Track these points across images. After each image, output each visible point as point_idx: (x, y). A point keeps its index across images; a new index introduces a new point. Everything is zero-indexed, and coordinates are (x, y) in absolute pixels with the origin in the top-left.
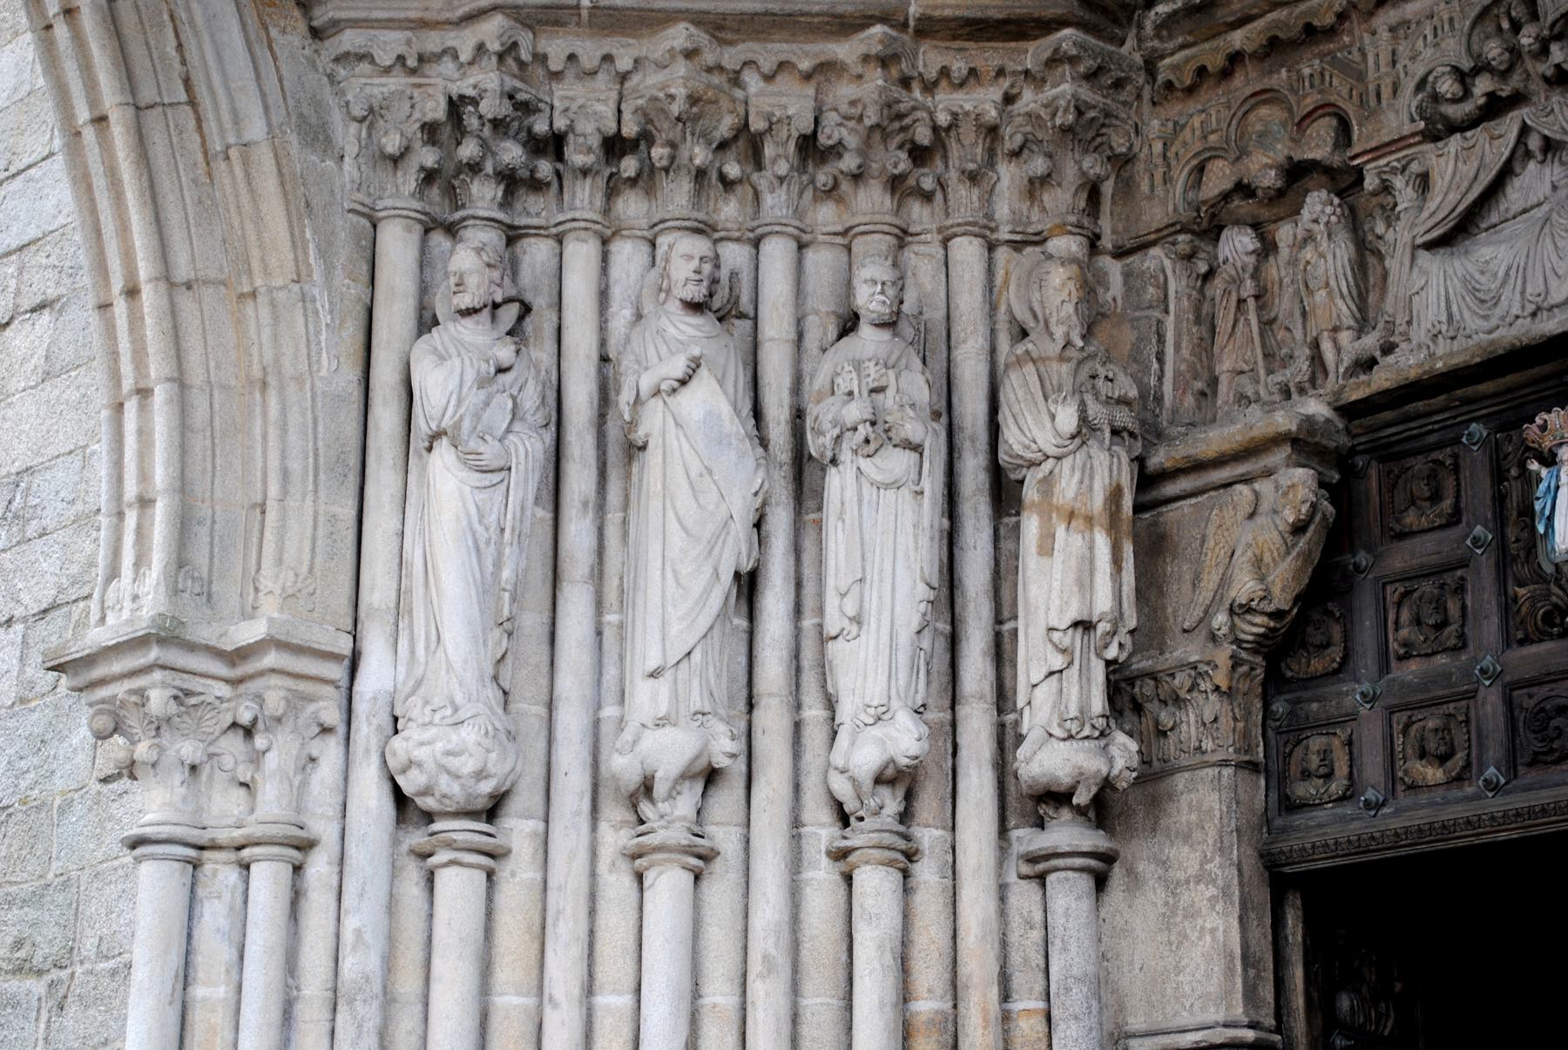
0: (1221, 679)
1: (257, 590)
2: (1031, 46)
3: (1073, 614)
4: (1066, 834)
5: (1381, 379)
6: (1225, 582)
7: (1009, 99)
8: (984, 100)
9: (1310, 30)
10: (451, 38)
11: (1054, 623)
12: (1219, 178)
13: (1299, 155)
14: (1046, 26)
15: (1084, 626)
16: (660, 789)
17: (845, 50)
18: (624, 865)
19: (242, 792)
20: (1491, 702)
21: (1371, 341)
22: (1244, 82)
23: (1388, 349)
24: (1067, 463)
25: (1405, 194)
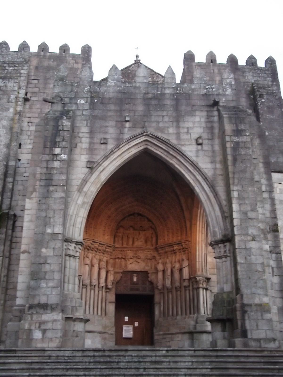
4: (108, 290)
10: (88, 241)
12: (117, 257)
14: (112, 247)
17: (103, 246)
25: (128, 261)
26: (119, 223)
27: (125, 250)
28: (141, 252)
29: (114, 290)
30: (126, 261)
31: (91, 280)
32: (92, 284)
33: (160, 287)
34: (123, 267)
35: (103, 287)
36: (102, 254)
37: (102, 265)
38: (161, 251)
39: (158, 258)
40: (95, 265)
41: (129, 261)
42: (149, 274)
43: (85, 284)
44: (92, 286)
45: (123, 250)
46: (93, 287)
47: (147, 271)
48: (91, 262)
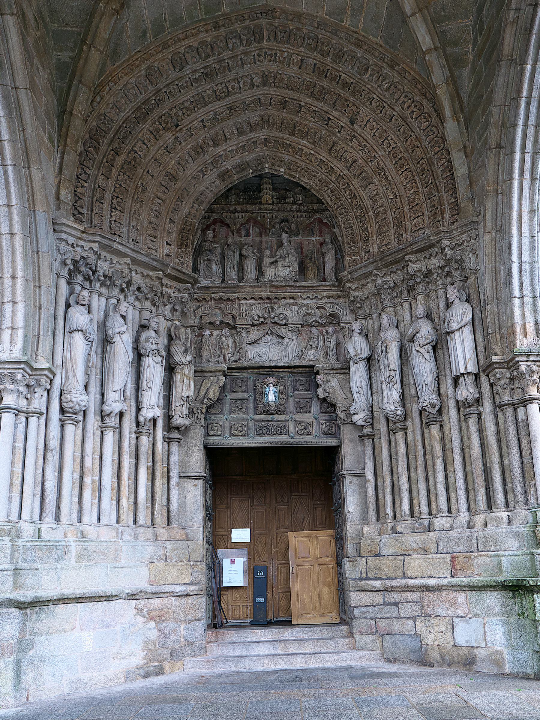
0: (204, 411)
1: (37, 355)
2: (181, 284)
3: (187, 395)
4: (175, 435)
5: (238, 365)
6: (207, 393)
7: (174, 292)
8: (171, 291)
9: (229, 298)
11: (183, 395)
12: (206, 320)
13: (225, 320)
14: (187, 282)
15: (188, 397)
16: (113, 414)
18: (100, 429)
19: (26, 400)
20: (251, 424)
21: (236, 357)
22: (212, 303)
23: (240, 360)
24: (186, 366)
25: (244, 333)
26: (210, 210)
27: (233, 296)
28: (288, 301)
29: (199, 432)
30: (239, 333)
31: (102, 394)
32: (107, 408)
33: (359, 418)
34: (228, 357)
35: (154, 421)
36: (148, 304)
37: (147, 341)
38: (359, 294)
39: (346, 317)
40: (117, 339)
41: (248, 332)
42: (317, 373)
43: (71, 404)
44: (109, 415)
45: (225, 296)
46: (113, 421)
47: (311, 363)
48: (103, 327)
